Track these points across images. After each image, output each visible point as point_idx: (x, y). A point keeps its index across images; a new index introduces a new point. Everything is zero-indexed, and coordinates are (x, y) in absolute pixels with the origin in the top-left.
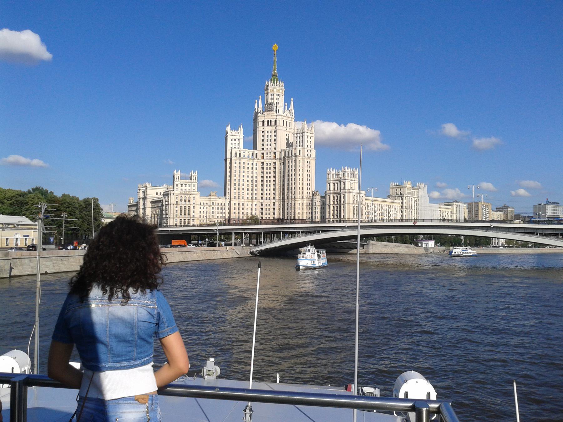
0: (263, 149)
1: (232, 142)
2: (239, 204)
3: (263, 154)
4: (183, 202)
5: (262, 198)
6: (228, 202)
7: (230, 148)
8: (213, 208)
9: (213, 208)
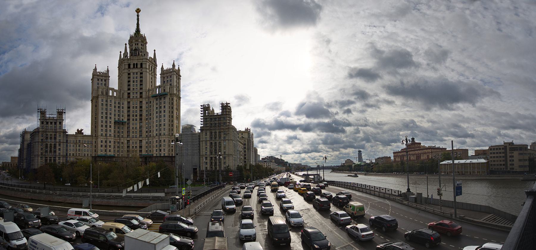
0: (129, 89)
1: (98, 82)
2: (106, 142)
3: (129, 94)
4: (49, 140)
5: (128, 136)
6: (94, 140)
7: (97, 88)
8: (79, 146)
9: (79, 146)
